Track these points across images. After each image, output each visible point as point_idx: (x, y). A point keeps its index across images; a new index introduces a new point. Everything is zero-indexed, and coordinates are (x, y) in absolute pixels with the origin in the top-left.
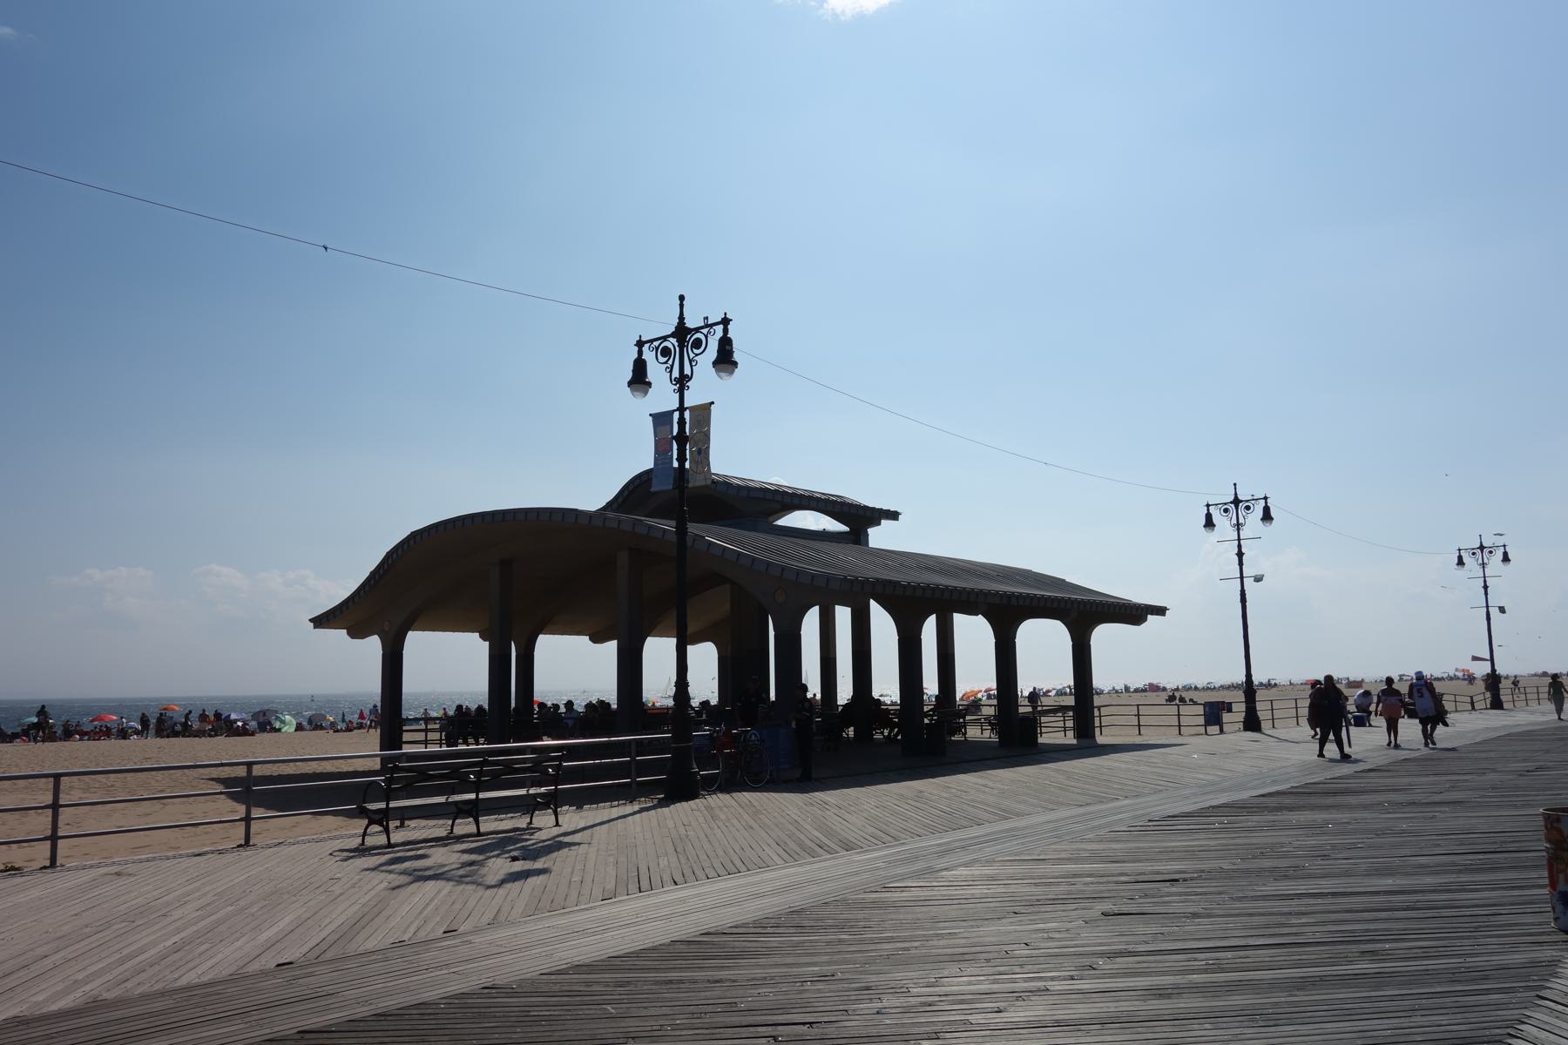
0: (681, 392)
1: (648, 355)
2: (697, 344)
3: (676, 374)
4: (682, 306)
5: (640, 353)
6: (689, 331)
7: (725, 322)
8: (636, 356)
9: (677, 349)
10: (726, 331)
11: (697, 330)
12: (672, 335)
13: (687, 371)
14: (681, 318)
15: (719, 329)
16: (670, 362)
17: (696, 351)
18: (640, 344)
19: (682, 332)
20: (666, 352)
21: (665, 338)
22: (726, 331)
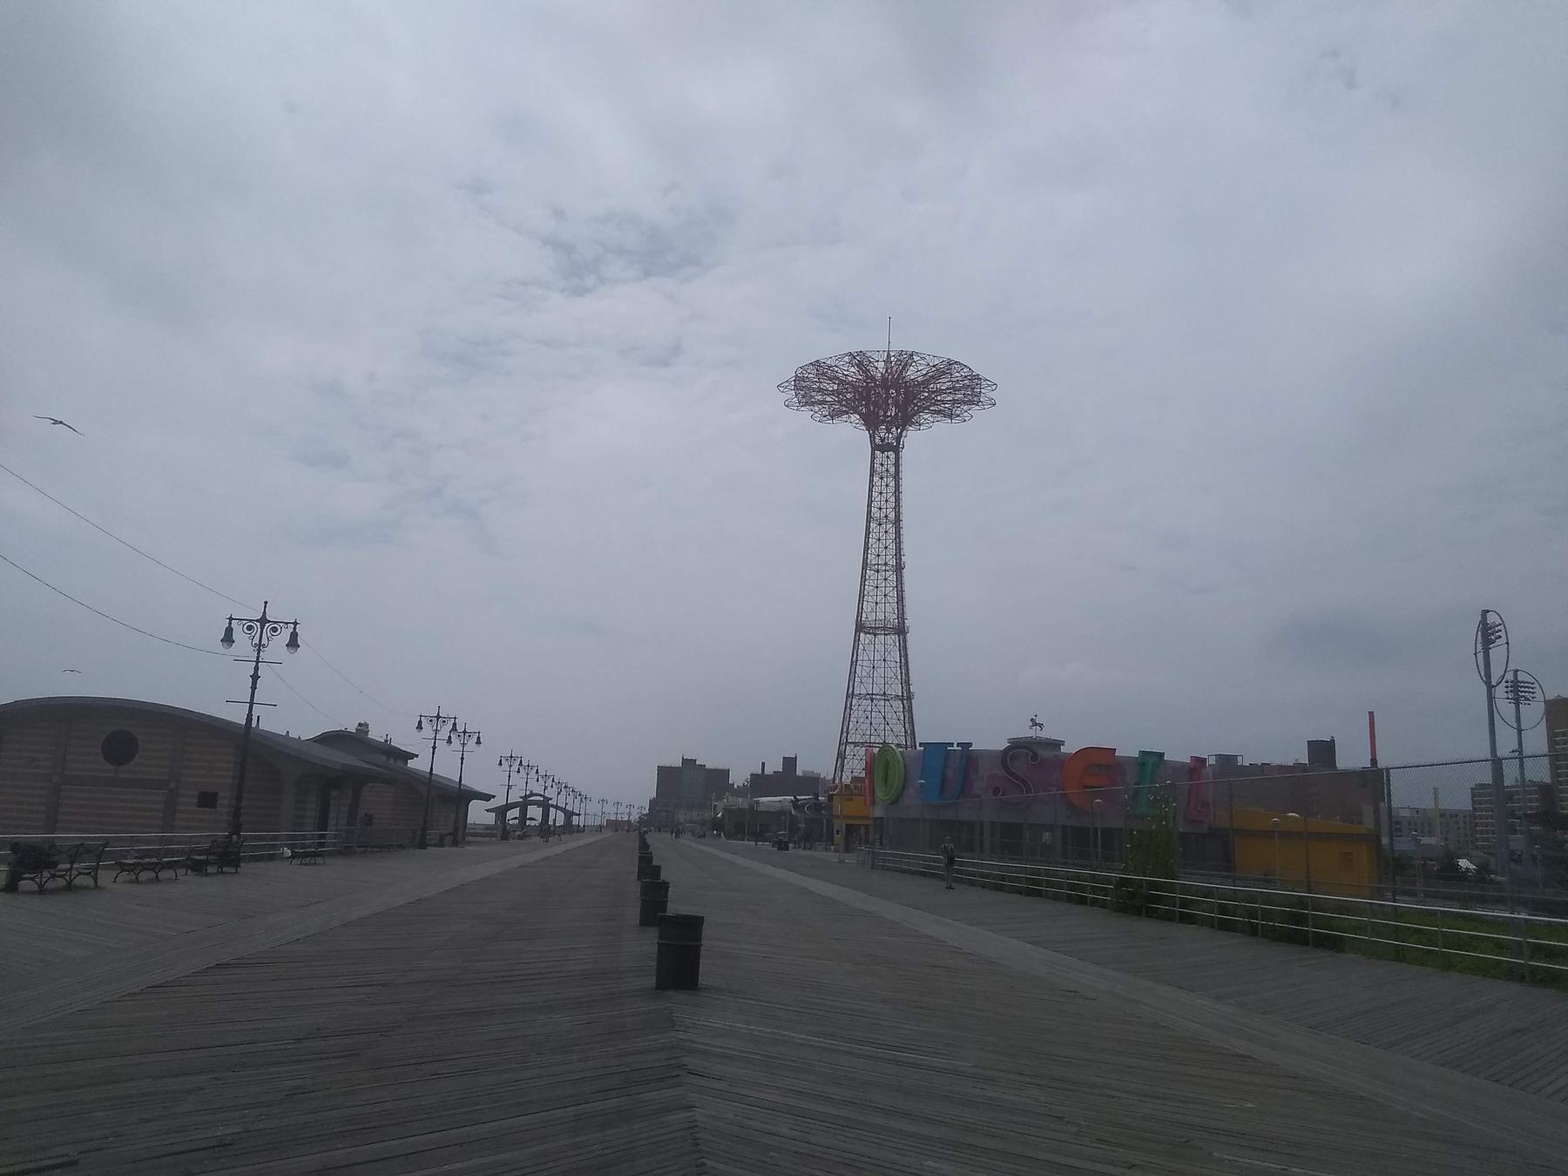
2: (275, 630)
3: (256, 640)
4: (265, 607)
5: (230, 623)
6: (270, 622)
7: (295, 623)
9: (259, 630)
10: (295, 628)
11: (276, 622)
12: (257, 621)
13: (264, 641)
16: (253, 634)
18: (231, 619)
19: (263, 621)
20: (250, 628)
21: (251, 621)
22: (295, 628)
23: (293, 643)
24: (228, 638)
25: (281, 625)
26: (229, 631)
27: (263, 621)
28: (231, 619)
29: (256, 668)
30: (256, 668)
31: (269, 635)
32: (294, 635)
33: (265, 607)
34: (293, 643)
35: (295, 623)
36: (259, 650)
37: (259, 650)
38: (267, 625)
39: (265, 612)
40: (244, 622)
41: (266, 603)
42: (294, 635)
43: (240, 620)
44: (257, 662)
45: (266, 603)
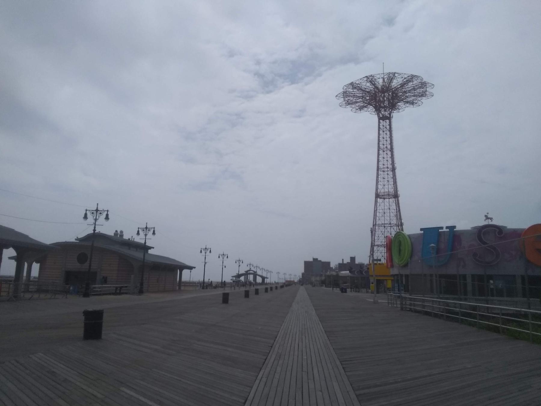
0: (96, 221)
2: (101, 213)
3: (95, 218)
4: (97, 206)
6: (99, 211)
7: (108, 211)
8: (85, 212)
10: (107, 213)
11: (101, 211)
12: (95, 210)
14: (97, 208)
17: (101, 215)
18: (86, 210)
20: (93, 213)
21: (93, 211)
22: (107, 213)
23: (107, 218)
24: (86, 217)
25: (103, 211)
26: (86, 215)
28: (86, 210)
29: (95, 227)
30: (95, 227)
32: (107, 215)
33: (97, 206)
34: (107, 218)
35: (108, 211)
36: (96, 221)
38: (98, 212)
39: (97, 208)
40: (91, 211)
41: (98, 204)
42: (107, 215)
43: (89, 210)
44: (95, 225)
45: (98, 204)
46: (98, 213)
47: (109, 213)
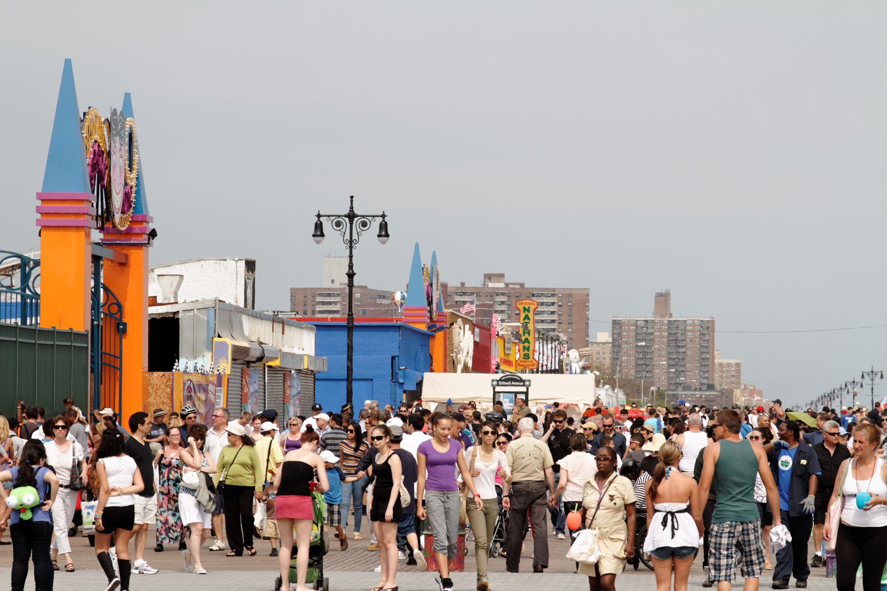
1: (322, 219)
2: (364, 224)
3: (347, 237)
6: (357, 216)
7: (383, 216)
11: (364, 216)
12: (345, 216)
13: (355, 237)
14: (352, 208)
15: (381, 219)
19: (351, 216)
20: (338, 224)
21: (339, 216)
25: (370, 218)
27: (351, 216)
28: (319, 216)
31: (359, 230)
32: (384, 227)
35: (383, 216)
36: (351, 247)
37: (351, 247)
38: (356, 219)
39: (352, 208)
40: (332, 218)
41: (352, 197)
42: (384, 227)
43: (329, 216)
45: (352, 197)
46: (355, 222)
47: (386, 219)
